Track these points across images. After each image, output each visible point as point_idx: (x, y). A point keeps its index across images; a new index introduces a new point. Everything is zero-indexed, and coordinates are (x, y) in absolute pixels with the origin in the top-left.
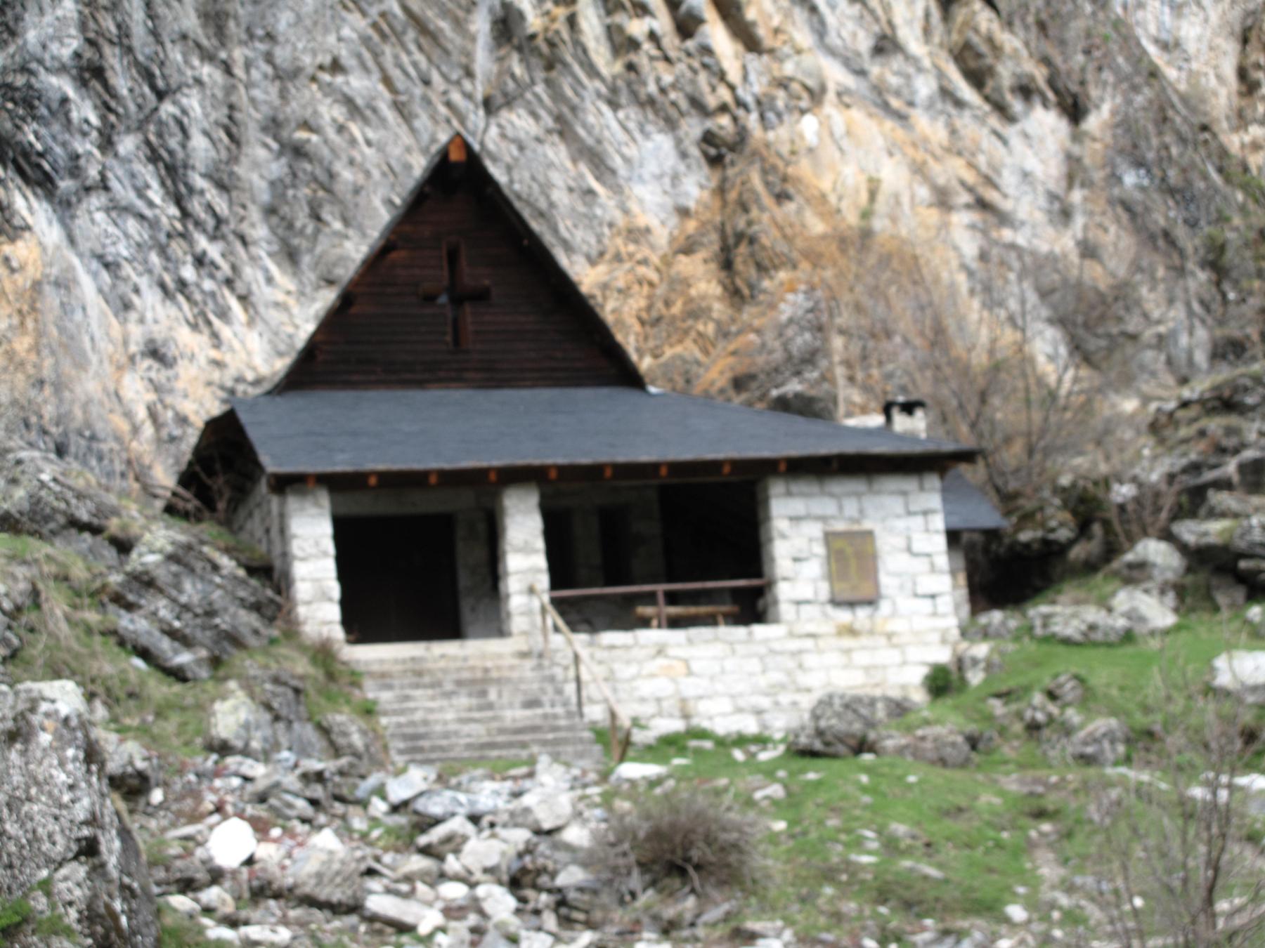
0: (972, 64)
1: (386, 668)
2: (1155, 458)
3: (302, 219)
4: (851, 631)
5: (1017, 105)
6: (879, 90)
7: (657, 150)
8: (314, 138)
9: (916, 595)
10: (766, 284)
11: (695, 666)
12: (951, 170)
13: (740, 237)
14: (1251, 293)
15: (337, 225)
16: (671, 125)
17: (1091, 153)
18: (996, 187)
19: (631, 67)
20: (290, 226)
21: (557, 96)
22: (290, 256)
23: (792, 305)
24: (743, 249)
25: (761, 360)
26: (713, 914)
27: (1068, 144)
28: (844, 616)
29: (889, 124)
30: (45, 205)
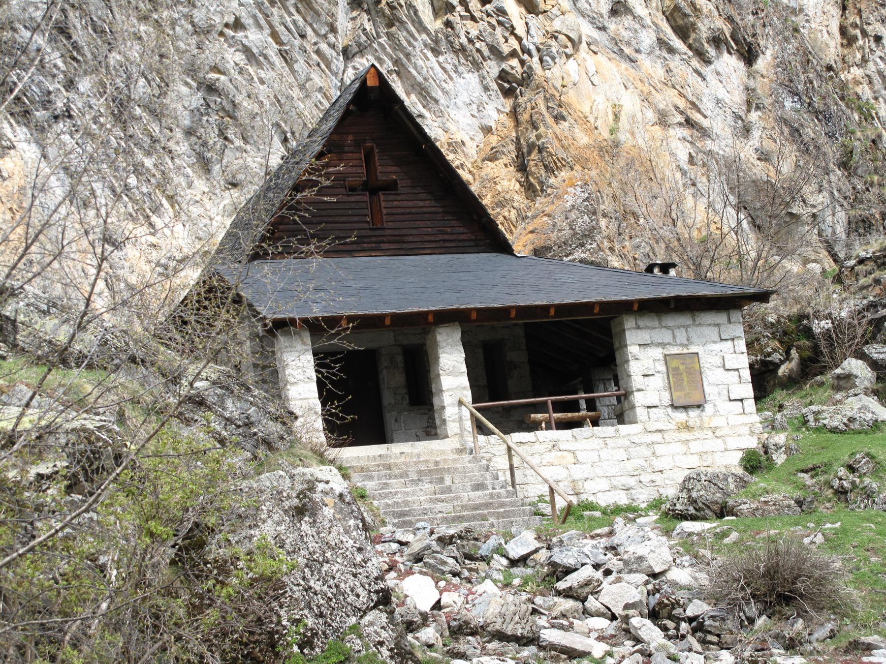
0: (680, 22)
1: (362, 463)
2: (841, 302)
3: (213, 137)
4: (688, 428)
5: (712, 52)
6: (615, 41)
7: (467, 85)
8: (223, 78)
9: (730, 400)
10: (552, 180)
11: (581, 456)
12: (667, 99)
13: (531, 147)
14: (872, 185)
15: (238, 143)
16: (477, 66)
17: (762, 86)
18: (699, 110)
19: (448, 24)
20: (205, 144)
21: (396, 45)
22: (205, 165)
23: (573, 196)
24: (534, 155)
25: (554, 236)
26: (822, 633)
27: (745, 79)
28: (681, 416)
29: (624, 65)
30: (25, 129)
